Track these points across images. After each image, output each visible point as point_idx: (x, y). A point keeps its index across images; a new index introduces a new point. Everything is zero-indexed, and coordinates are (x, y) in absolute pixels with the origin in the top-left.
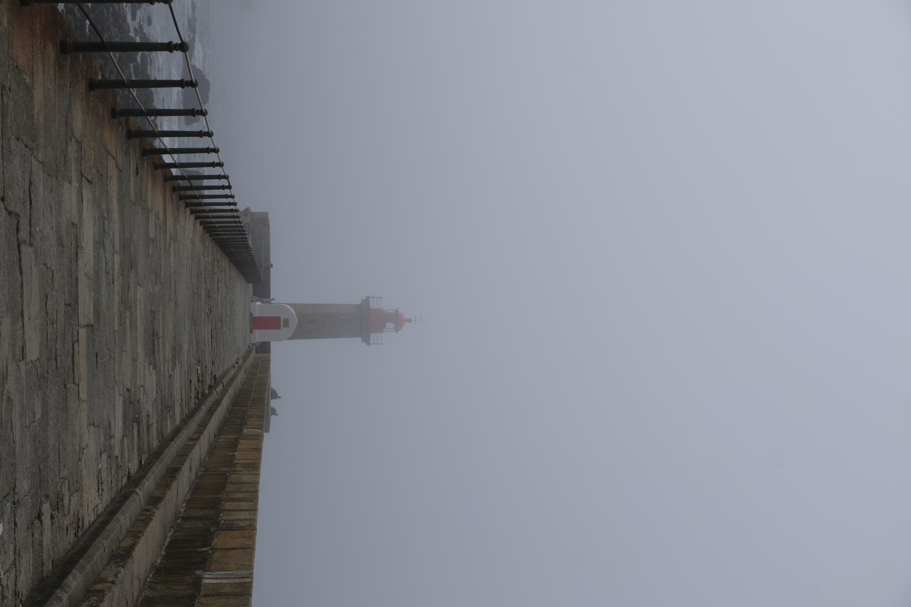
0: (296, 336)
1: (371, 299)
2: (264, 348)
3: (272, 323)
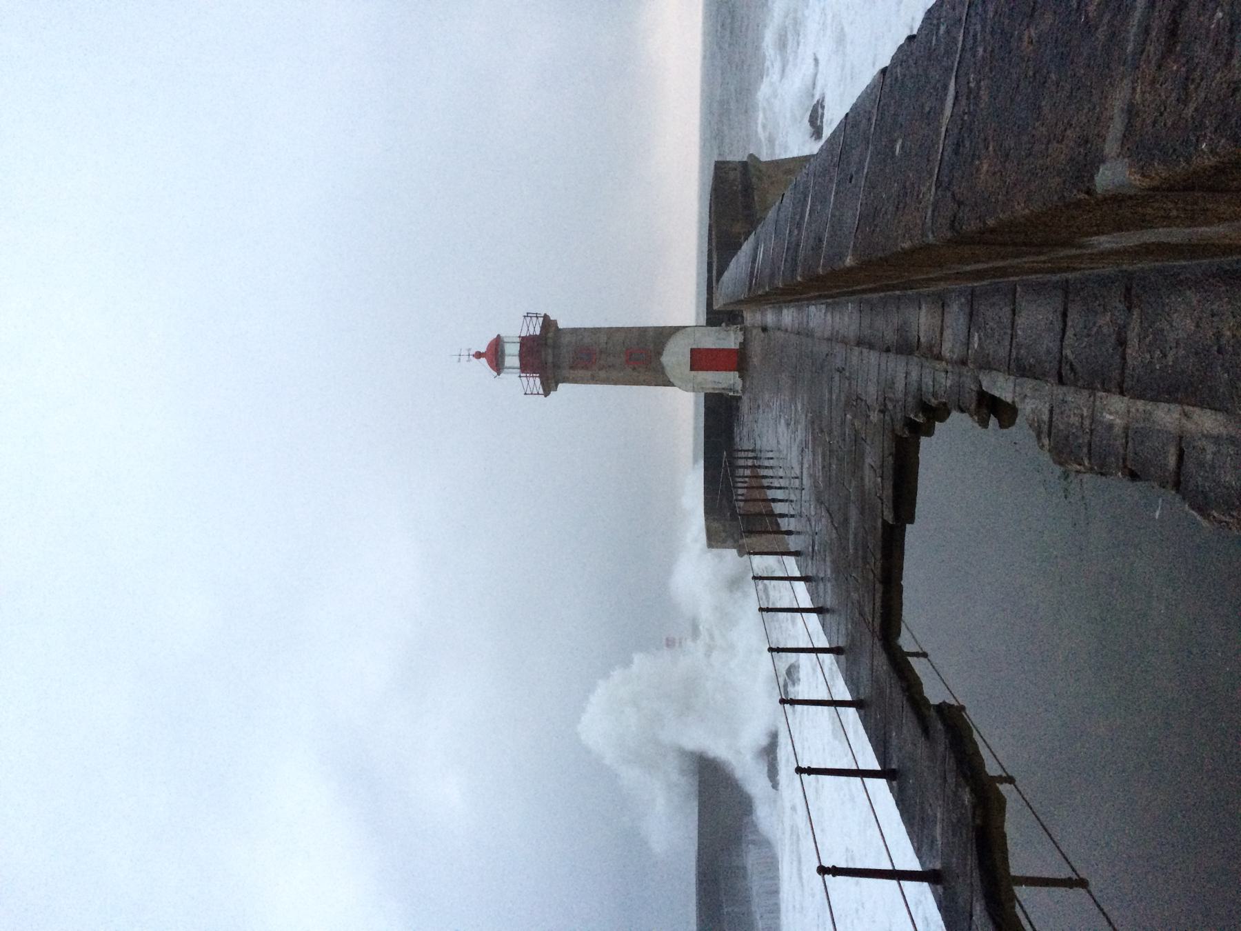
0: (664, 335)
1: (541, 391)
2: (715, 317)
3: (701, 360)
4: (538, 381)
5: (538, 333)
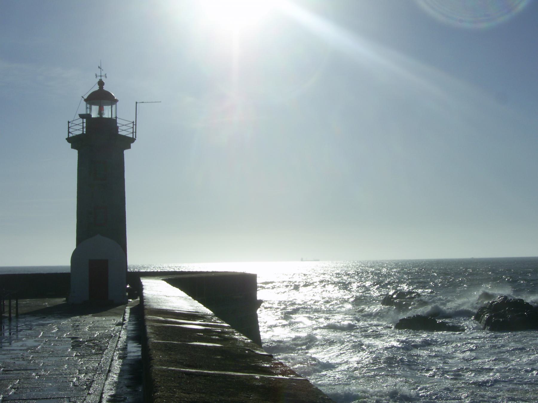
1: (71, 135)
5: (121, 133)
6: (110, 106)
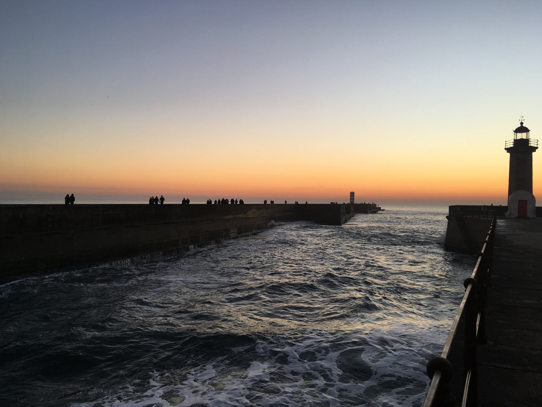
4: (512, 146)
5: (531, 145)
6: (525, 133)
